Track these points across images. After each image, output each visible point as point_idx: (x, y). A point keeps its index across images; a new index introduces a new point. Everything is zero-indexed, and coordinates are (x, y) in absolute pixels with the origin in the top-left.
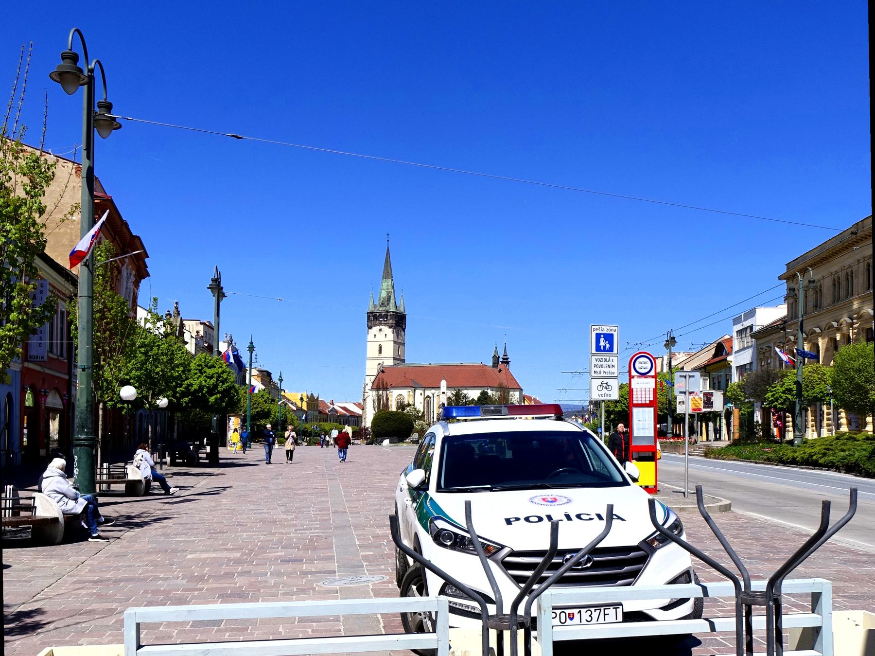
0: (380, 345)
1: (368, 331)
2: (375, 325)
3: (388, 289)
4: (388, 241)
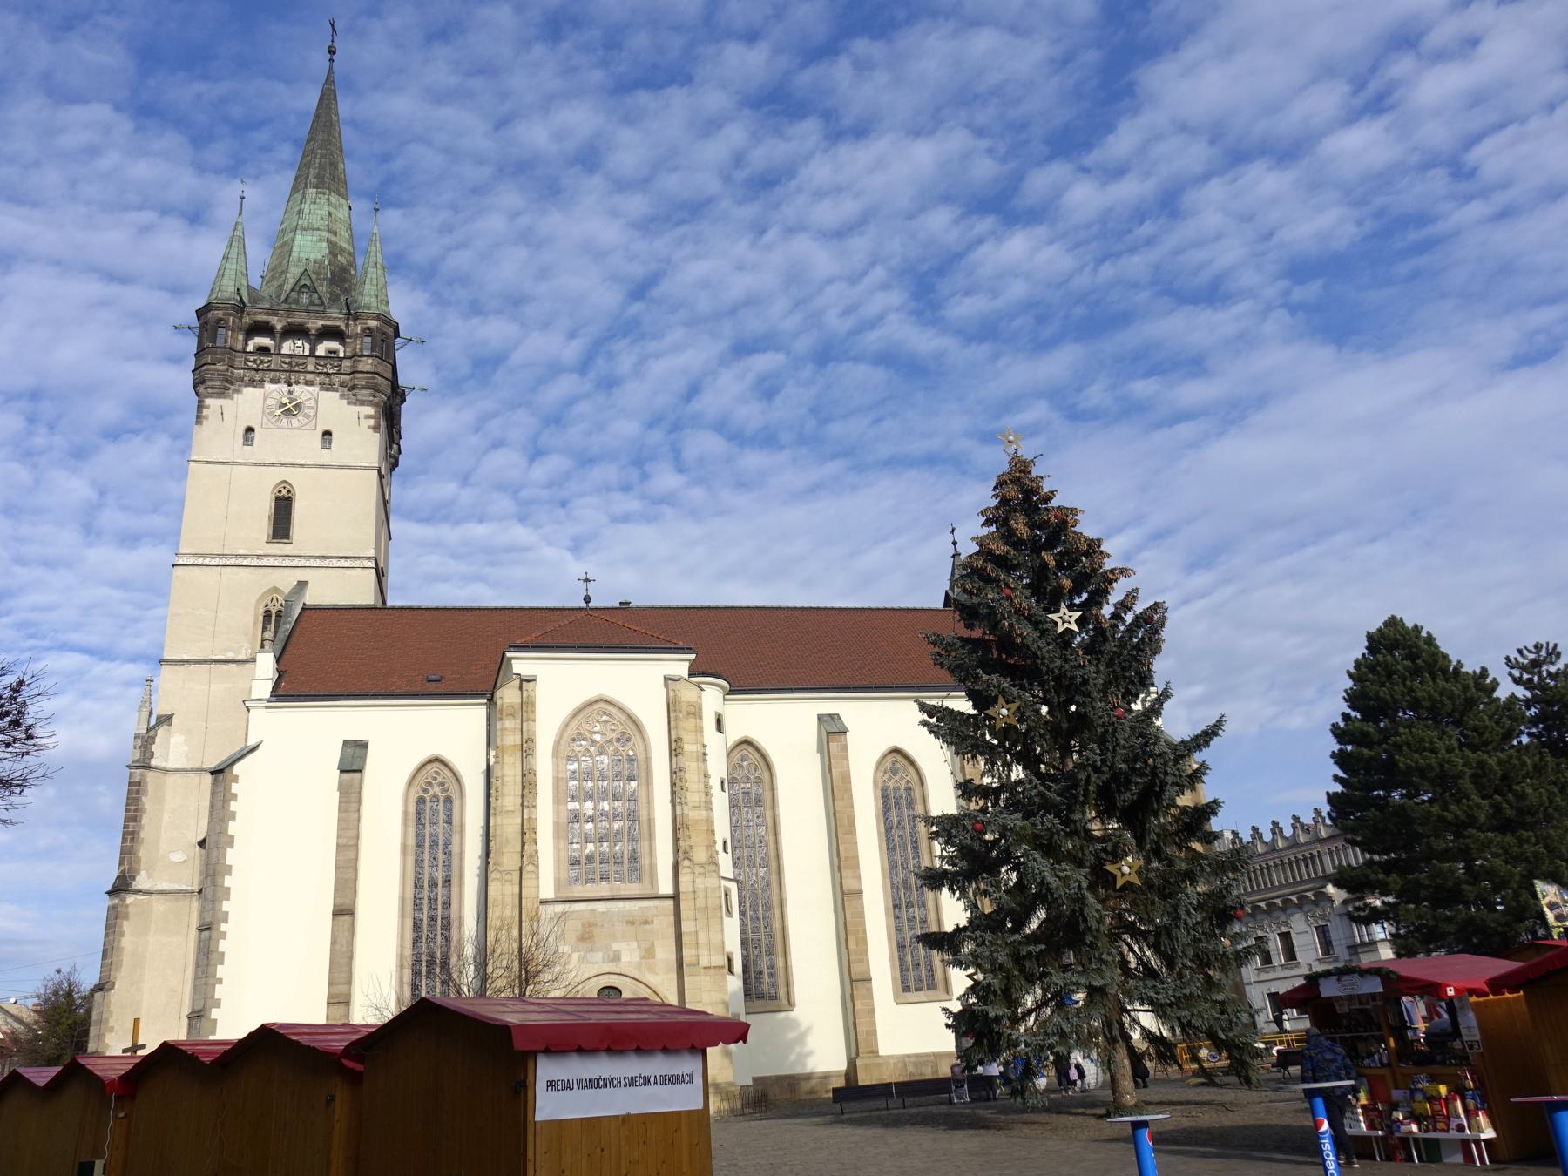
1: (201, 406)
3: (335, 234)
4: (332, 52)
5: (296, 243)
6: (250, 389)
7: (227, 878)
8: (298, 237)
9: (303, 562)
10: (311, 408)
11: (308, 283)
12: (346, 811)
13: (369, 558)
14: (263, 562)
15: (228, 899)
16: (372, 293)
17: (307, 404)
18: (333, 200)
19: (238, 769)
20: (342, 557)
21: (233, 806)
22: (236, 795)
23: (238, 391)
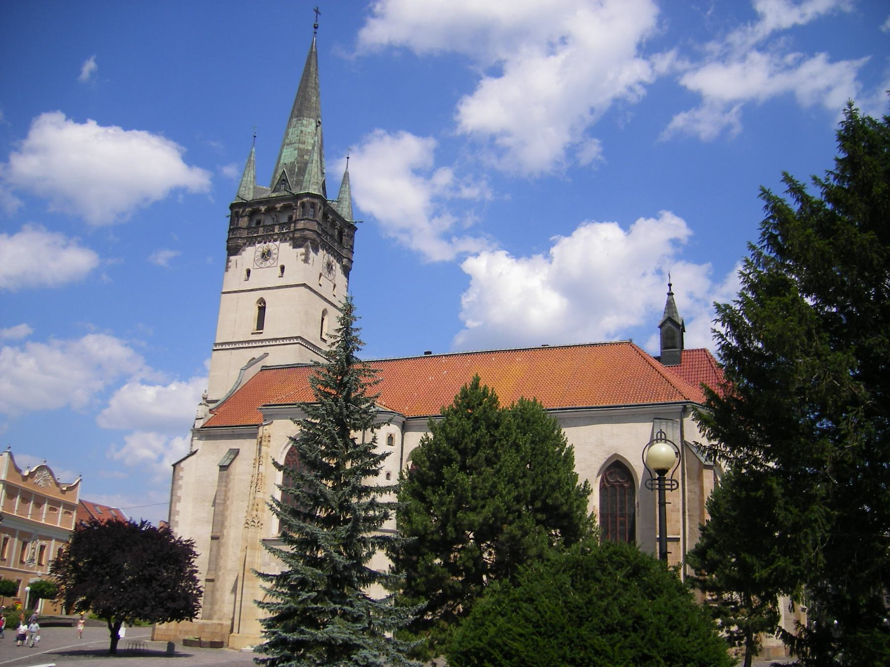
0: (262, 301)
1: (228, 261)
2: (251, 241)
4: (316, 28)
5: (284, 154)
6: (250, 248)
7: (176, 517)
8: (285, 150)
9: (267, 343)
10: (275, 254)
11: (285, 178)
12: (221, 486)
13: (297, 338)
14: (250, 345)
15: (177, 527)
16: (308, 179)
17: (274, 252)
18: (305, 122)
19: (183, 464)
20: (283, 339)
21: (180, 482)
22: (182, 477)
23: (244, 250)
